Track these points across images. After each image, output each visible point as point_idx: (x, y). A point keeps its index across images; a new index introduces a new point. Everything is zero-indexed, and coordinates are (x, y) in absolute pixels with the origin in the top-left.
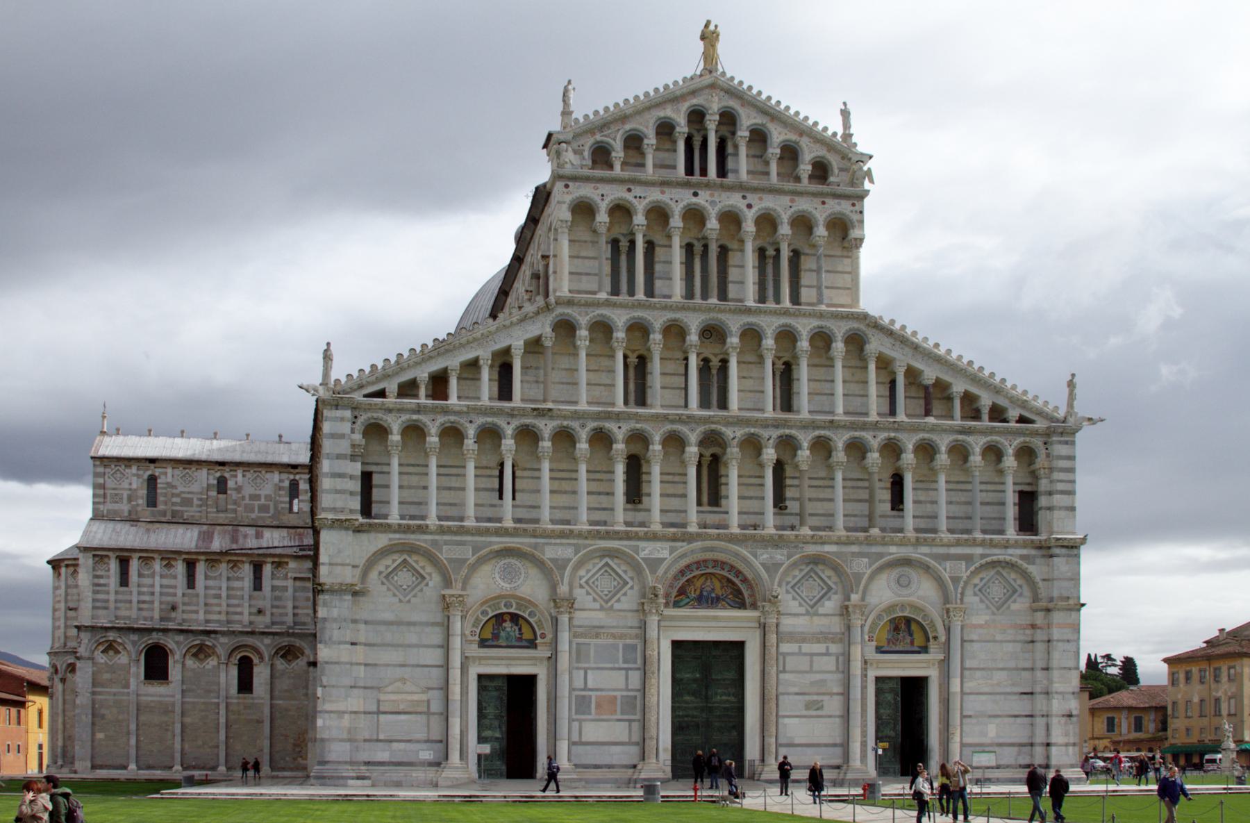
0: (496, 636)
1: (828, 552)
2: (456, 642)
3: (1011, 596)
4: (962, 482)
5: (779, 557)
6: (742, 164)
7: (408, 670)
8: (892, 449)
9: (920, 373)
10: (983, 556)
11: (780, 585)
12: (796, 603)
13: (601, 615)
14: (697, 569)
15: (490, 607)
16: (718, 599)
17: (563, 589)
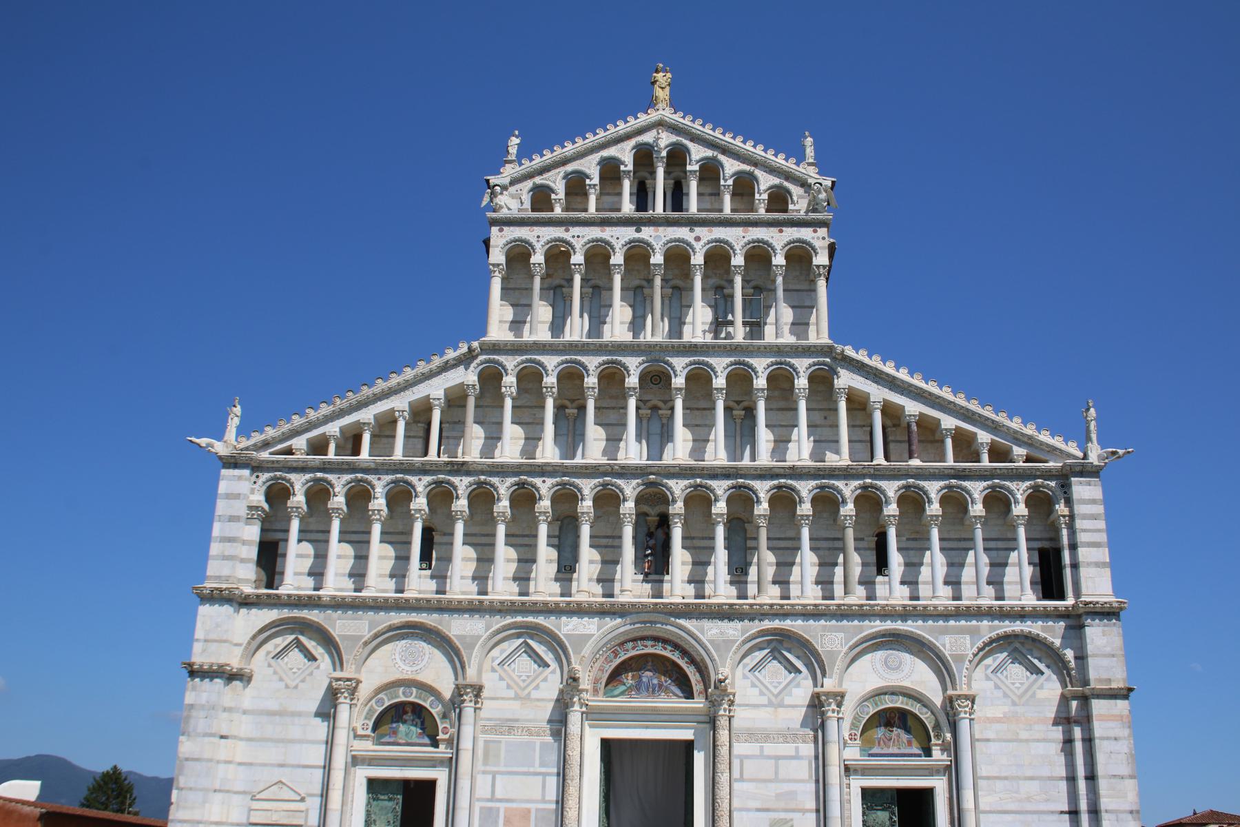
0: (395, 732)
1: (792, 626)
2: (342, 736)
3: (1035, 681)
4: (965, 539)
5: (731, 632)
6: (693, 205)
7: (286, 770)
8: (870, 502)
10: (992, 629)
11: (733, 670)
12: (756, 691)
13: (516, 705)
14: (633, 648)
15: (386, 695)
16: (660, 686)
17: (471, 674)
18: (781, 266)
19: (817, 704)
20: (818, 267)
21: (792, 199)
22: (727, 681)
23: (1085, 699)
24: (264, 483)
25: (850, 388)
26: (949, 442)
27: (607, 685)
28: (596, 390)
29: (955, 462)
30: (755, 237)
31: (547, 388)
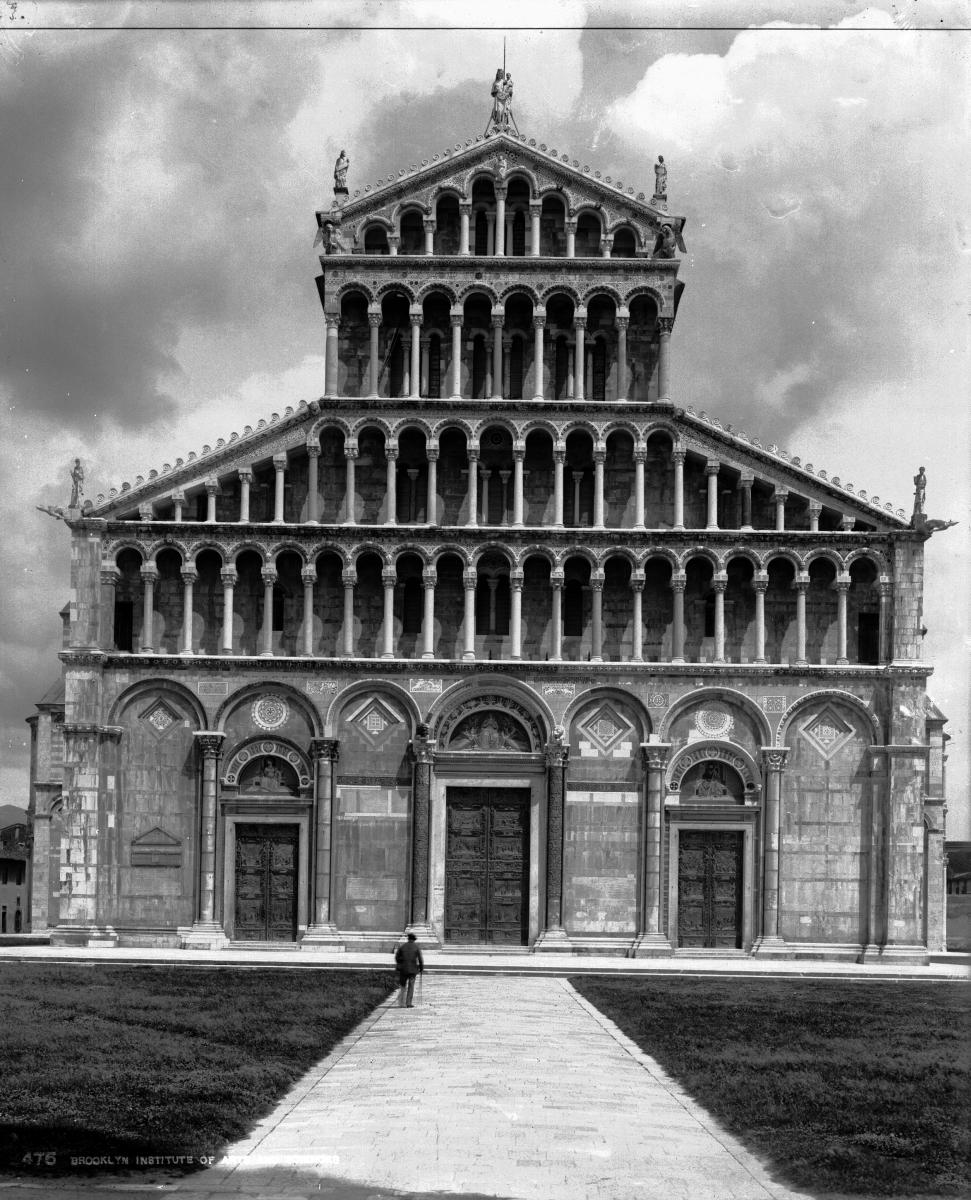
3: (845, 737)
5: (566, 691)
8: (700, 568)
9: (737, 473)
18: (625, 318)
19: (643, 755)
20: (663, 319)
21: (639, 239)
22: (562, 737)
23: (886, 757)
24: (115, 548)
25: (689, 452)
26: (781, 509)
27: (451, 739)
28: (438, 453)
29: (786, 528)
30: (599, 285)
31: (389, 450)
